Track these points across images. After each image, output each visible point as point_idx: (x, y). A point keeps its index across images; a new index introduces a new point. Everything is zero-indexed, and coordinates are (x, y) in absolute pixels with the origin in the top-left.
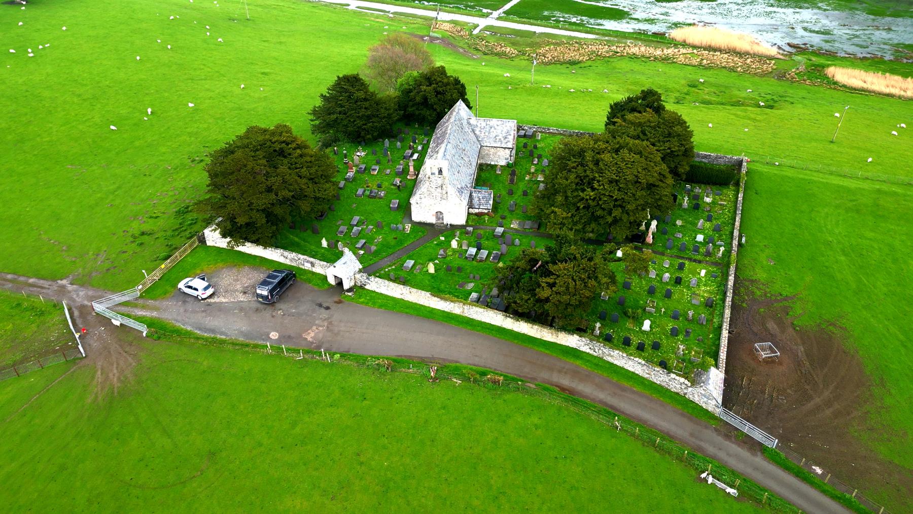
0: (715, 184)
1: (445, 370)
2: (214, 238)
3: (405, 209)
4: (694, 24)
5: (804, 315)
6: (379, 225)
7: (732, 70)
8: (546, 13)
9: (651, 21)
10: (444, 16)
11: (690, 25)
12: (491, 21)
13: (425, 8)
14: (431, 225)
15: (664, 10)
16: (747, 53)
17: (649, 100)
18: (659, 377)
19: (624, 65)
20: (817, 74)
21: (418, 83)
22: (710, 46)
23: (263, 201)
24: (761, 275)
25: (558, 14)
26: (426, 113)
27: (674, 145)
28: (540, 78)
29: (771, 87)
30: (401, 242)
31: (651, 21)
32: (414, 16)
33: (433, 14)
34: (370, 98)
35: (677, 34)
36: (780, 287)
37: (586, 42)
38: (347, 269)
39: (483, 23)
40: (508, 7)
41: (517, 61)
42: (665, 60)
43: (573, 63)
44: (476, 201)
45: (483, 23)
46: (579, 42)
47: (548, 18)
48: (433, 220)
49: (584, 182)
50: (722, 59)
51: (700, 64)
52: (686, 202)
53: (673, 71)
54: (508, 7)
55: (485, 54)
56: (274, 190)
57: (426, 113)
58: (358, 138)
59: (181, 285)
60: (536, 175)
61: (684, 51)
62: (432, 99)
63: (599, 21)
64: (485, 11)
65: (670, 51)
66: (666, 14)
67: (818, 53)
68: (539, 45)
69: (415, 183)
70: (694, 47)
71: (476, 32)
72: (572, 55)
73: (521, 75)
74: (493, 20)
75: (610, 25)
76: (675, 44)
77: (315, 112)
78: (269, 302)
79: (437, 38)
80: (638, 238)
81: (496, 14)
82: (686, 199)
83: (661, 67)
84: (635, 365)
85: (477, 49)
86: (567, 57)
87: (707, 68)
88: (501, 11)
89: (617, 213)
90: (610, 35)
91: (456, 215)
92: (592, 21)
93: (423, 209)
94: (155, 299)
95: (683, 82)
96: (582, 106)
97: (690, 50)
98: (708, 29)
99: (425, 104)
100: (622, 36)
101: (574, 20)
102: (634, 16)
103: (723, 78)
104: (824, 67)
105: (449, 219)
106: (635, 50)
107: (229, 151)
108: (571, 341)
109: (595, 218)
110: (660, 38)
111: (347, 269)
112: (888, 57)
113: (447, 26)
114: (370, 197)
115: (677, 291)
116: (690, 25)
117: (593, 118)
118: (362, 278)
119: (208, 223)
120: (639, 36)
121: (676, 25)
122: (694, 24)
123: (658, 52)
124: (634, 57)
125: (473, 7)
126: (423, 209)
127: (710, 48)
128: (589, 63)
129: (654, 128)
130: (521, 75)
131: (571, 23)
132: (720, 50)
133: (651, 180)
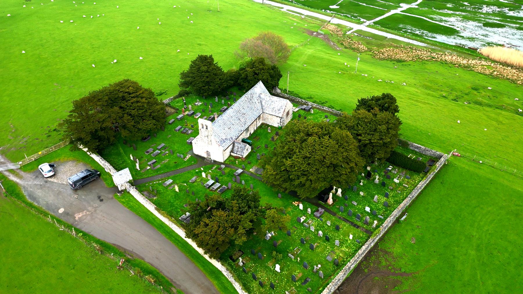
0: (410, 170)
1: (130, 261)
4: (503, 46)
6: (172, 153)
7: (513, 81)
8: (401, 26)
9: (472, 39)
11: (500, 45)
12: (363, 27)
14: (203, 158)
15: (485, 33)
19: (432, 67)
22: (505, 62)
24: (397, 249)
25: (409, 27)
30: (176, 166)
31: (472, 39)
32: (317, 19)
35: (485, 51)
36: (405, 265)
37: (417, 48)
38: (122, 178)
39: (356, 27)
40: (377, 19)
41: (363, 54)
42: (467, 68)
43: (399, 61)
44: (236, 148)
45: (356, 27)
46: (412, 47)
47: (400, 29)
48: (205, 156)
50: (510, 72)
51: (491, 74)
53: (467, 76)
54: (377, 19)
55: (346, 48)
61: (484, 63)
63: (435, 35)
64: (362, 20)
66: (486, 36)
68: (384, 46)
70: (494, 61)
71: (348, 33)
72: (402, 56)
74: (366, 26)
75: (441, 38)
76: (481, 57)
77: (184, 75)
79: (322, 34)
81: (368, 23)
82: (377, 177)
83: (459, 72)
85: (342, 44)
86: (398, 57)
87: (496, 78)
88: (373, 21)
89: (303, 179)
90: (436, 45)
92: (430, 34)
94: (24, 171)
95: (469, 85)
97: (489, 63)
98: (513, 50)
100: (445, 46)
101: (418, 32)
102: (461, 34)
103: (503, 86)
105: (214, 157)
106: (448, 58)
108: (217, 264)
110: (473, 52)
113: (332, 27)
114: (182, 132)
116: (500, 45)
118: (128, 186)
120: (459, 49)
121: (489, 44)
122: (503, 46)
123: (465, 62)
124: (445, 63)
125: (355, 17)
127: (505, 64)
128: (411, 62)
129: (366, 123)
131: (414, 35)
132: (512, 66)
133: (335, 162)
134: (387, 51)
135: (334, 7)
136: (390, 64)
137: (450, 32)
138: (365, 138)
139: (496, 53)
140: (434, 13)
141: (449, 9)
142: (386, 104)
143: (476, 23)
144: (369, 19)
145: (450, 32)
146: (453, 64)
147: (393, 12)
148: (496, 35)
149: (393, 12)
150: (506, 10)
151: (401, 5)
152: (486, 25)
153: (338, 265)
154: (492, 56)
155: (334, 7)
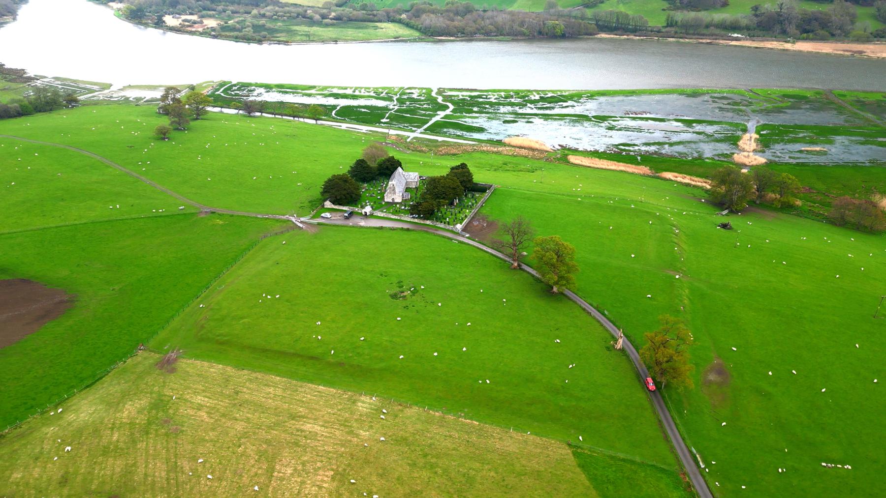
2: (328, 204)
3: (383, 198)
5: (490, 219)
7: (526, 157)
10: (392, 132)
13: (382, 127)
16: (537, 149)
17: (463, 166)
18: (448, 227)
20: (564, 159)
21: (384, 162)
23: (345, 192)
25: (451, 130)
26: (388, 172)
27: (465, 178)
28: (434, 161)
29: (541, 163)
32: (377, 132)
33: (386, 131)
34: (368, 166)
35: (507, 140)
38: (368, 209)
39: (412, 135)
42: (497, 153)
43: (454, 155)
45: (412, 135)
49: (435, 187)
52: (469, 195)
56: (349, 188)
57: (388, 172)
58: (364, 180)
59: (323, 215)
60: (423, 189)
62: (390, 167)
65: (500, 149)
66: (505, 130)
67: (570, 149)
69: (386, 191)
71: (408, 140)
72: (455, 151)
73: (427, 160)
74: (418, 133)
76: (505, 145)
78: (347, 218)
80: (452, 204)
81: (419, 130)
83: (494, 156)
84: (442, 226)
87: (515, 156)
96: (442, 168)
99: (388, 168)
103: (520, 160)
104: (567, 155)
106: (485, 148)
107: (330, 180)
108: (428, 222)
109: (438, 198)
110: (499, 142)
111: (368, 209)
112: (602, 150)
113: (394, 137)
115: (458, 215)
117: (445, 172)
119: (325, 200)
120: (490, 142)
126: (388, 199)
127: (521, 147)
130: (427, 160)
134: (443, 149)
135: (384, 120)
136: (449, 157)
137: (481, 130)
138: (461, 179)
139: (515, 141)
140: (466, 117)
141: (476, 112)
142: (463, 166)
143: (497, 122)
144: (419, 127)
145: (481, 130)
146: (488, 152)
147: (434, 120)
148: (512, 129)
149: (434, 120)
150: (517, 108)
151: (438, 113)
152: (505, 122)
153: (466, 216)
154: (513, 143)
155: (384, 120)
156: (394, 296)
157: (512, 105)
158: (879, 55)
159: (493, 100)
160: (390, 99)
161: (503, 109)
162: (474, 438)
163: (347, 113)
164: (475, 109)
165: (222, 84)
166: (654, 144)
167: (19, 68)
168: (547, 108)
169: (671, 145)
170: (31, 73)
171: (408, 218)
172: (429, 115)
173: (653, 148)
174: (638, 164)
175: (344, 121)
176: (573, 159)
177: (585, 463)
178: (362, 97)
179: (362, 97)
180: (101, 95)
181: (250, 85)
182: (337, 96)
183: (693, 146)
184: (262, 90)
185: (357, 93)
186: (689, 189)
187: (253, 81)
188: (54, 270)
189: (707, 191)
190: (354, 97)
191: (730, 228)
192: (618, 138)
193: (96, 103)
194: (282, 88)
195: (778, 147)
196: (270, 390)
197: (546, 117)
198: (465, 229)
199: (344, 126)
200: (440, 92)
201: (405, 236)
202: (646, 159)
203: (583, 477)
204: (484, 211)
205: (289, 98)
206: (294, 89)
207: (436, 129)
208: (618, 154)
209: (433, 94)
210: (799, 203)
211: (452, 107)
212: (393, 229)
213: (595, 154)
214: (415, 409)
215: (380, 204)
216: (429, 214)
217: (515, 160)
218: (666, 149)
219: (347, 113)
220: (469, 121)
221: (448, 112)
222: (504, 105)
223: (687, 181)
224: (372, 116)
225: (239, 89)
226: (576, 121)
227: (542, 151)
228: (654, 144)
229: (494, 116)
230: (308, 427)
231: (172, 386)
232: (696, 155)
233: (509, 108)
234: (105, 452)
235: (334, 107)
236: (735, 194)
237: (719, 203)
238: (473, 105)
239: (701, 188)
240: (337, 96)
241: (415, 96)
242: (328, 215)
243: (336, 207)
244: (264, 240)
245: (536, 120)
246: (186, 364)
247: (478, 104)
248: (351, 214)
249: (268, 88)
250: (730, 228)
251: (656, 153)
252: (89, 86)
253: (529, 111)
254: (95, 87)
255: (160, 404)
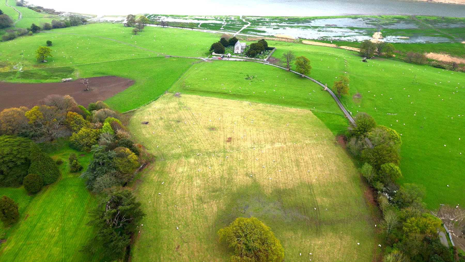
2: (214, 53)
17: (263, 40)
40: (240, 31)
46: (256, 37)
54: (240, 31)
56: (223, 46)
65: (274, 39)
67: (302, 39)
76: (275, 37)
84: (258, 59)
91: (240, 52)
93: (236, 52)
99: (233, 42)
100: (265, 36)
108: (253, 59)
110: (273, 36)
111: (229, 55)
126: (236, 52)
147: (243, 28)
150: (278, 24)
156: (247, 79)
157: (276, 22)
158: (439, 1)
159: (267, 20)
160: (222, 20)
161: (272, 24)
162: (281, 109)
163: (205, 26)
164: (260, 24)
165: (146, 15)
166: (338, 36)
167: (51, 8)
168: (291, 24)
169: (345, 37)
170: (57, 10)
171: (246, 58)
172: (240, 27)
173: (337, 38)
174: (331, 43)
175: (204, 29)
176: (304, 42)
177: (315, 114)
178: (209, 20)
179: (209, 20)
180: (95, 20)
181: (158, 15)
182: (198, 19)
183: (354, 37)
184: (164, 17)
185: (207, 18)
186: (352, 52)
187: (159, 14)
188: (123, 73)
189: (358, 52)
190: (206, 20)
191: (366, 62)
192: (323, 34)
193: (94, 23)
194: (172, 16)
195: (389, 37)
196: (215, 101)
197: (292, 27)
198: (267, 60)
199: (205, 31)
200: (244, 17)
201: (246, 63)
202: (334, 42)
203: (315, 116)
204: (274, 55)
205: (177, 20)
206: (178, 17)
207: (244, 31)
208: (323, 40)
209: (241, 18)
210: (394, 55)
211: (250, 23)
212: (240, 61)
213: (313, 40)
214: (261, 104)
215: (233, 53)
216: (253, 55)
217: (280, 42)
218: (343, 39)
219: (205, 26)
220: (258, 29)
221: (248, 25)
222: (272, 22)
223: (351, 48)
224: (216, 27)
225: (154, 17)
226: (305, 28)
227: (291, 39)
228: (338, 36)
229: (269, 27)
230: (229, 108)
231: (182, 100)
232: (355, 40)
233: (275, 24)
234: (170, 113)
235: (199, 24)
236: (368, 52)
237: (362, 55)
238: (259, 22)
239: (357, 51)
240: (198, 19)
241: (233, 19)
242: (215, 57)
243: (217, 54)
244: (194, 65)
245: (287, 28)
246: (182, 95)
247: (261, 22)
248: (223, 57)
249: (167, 16)
250: (366, 62)
251: (338, 40)
252: (87, 16)
253: (283, 24)
254: (90, 17)
255: (180, 103)
